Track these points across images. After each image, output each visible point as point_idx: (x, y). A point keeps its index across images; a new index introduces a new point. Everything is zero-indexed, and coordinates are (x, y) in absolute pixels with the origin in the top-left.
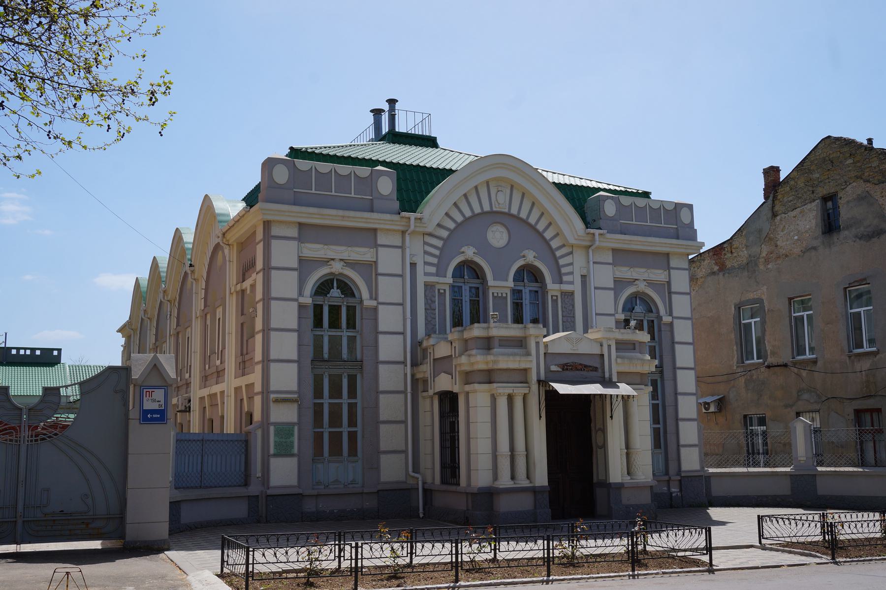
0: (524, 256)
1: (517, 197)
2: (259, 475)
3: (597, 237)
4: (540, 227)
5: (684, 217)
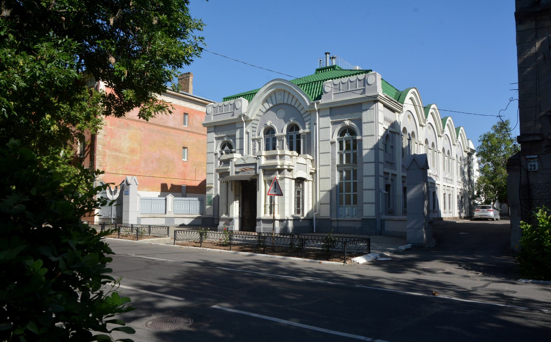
4: (296, 106)
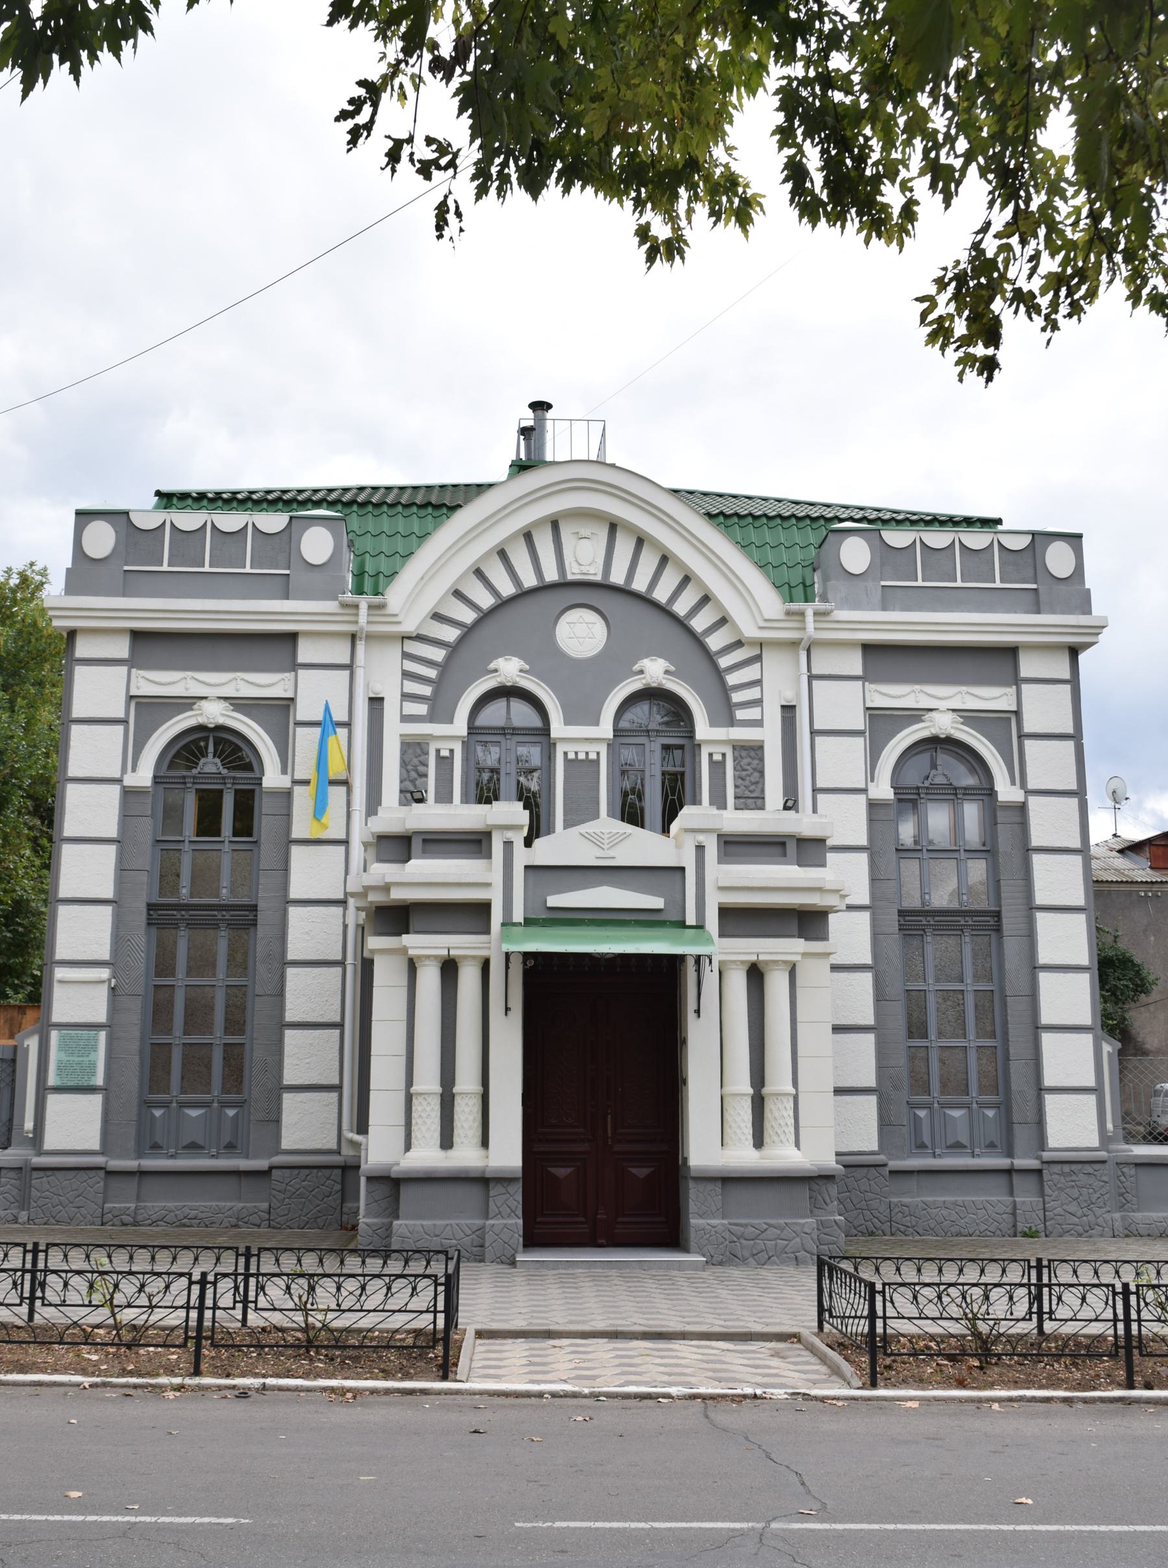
0: (642, 672)
1: (624, 548)
2: (29, 1125)
3: (810, 618)
4: (681, 608)
5: (1058, 560)
